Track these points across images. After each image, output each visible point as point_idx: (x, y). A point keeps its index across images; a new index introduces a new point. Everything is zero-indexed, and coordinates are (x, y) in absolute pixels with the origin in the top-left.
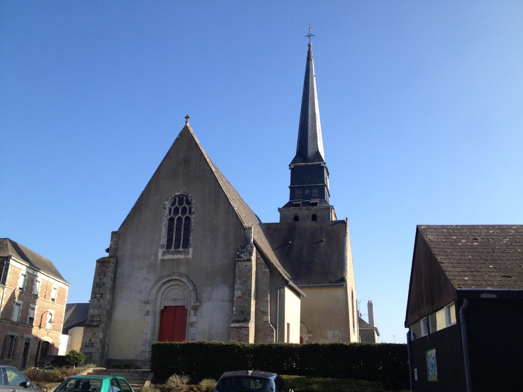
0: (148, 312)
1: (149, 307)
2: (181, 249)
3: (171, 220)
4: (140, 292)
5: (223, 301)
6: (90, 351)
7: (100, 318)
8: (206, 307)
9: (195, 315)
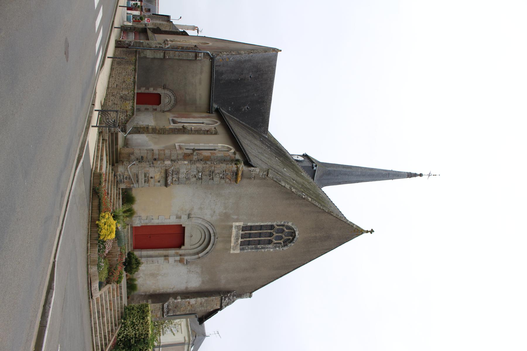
0: (180, 218)
1: (184, 217)
2: (241, 232)
3: (272, 227)
4: (201, 208)
5: (186, 283)
6: (140, 181)
7: (176, 180)
8: (182, 269)
9: (175, 261)
